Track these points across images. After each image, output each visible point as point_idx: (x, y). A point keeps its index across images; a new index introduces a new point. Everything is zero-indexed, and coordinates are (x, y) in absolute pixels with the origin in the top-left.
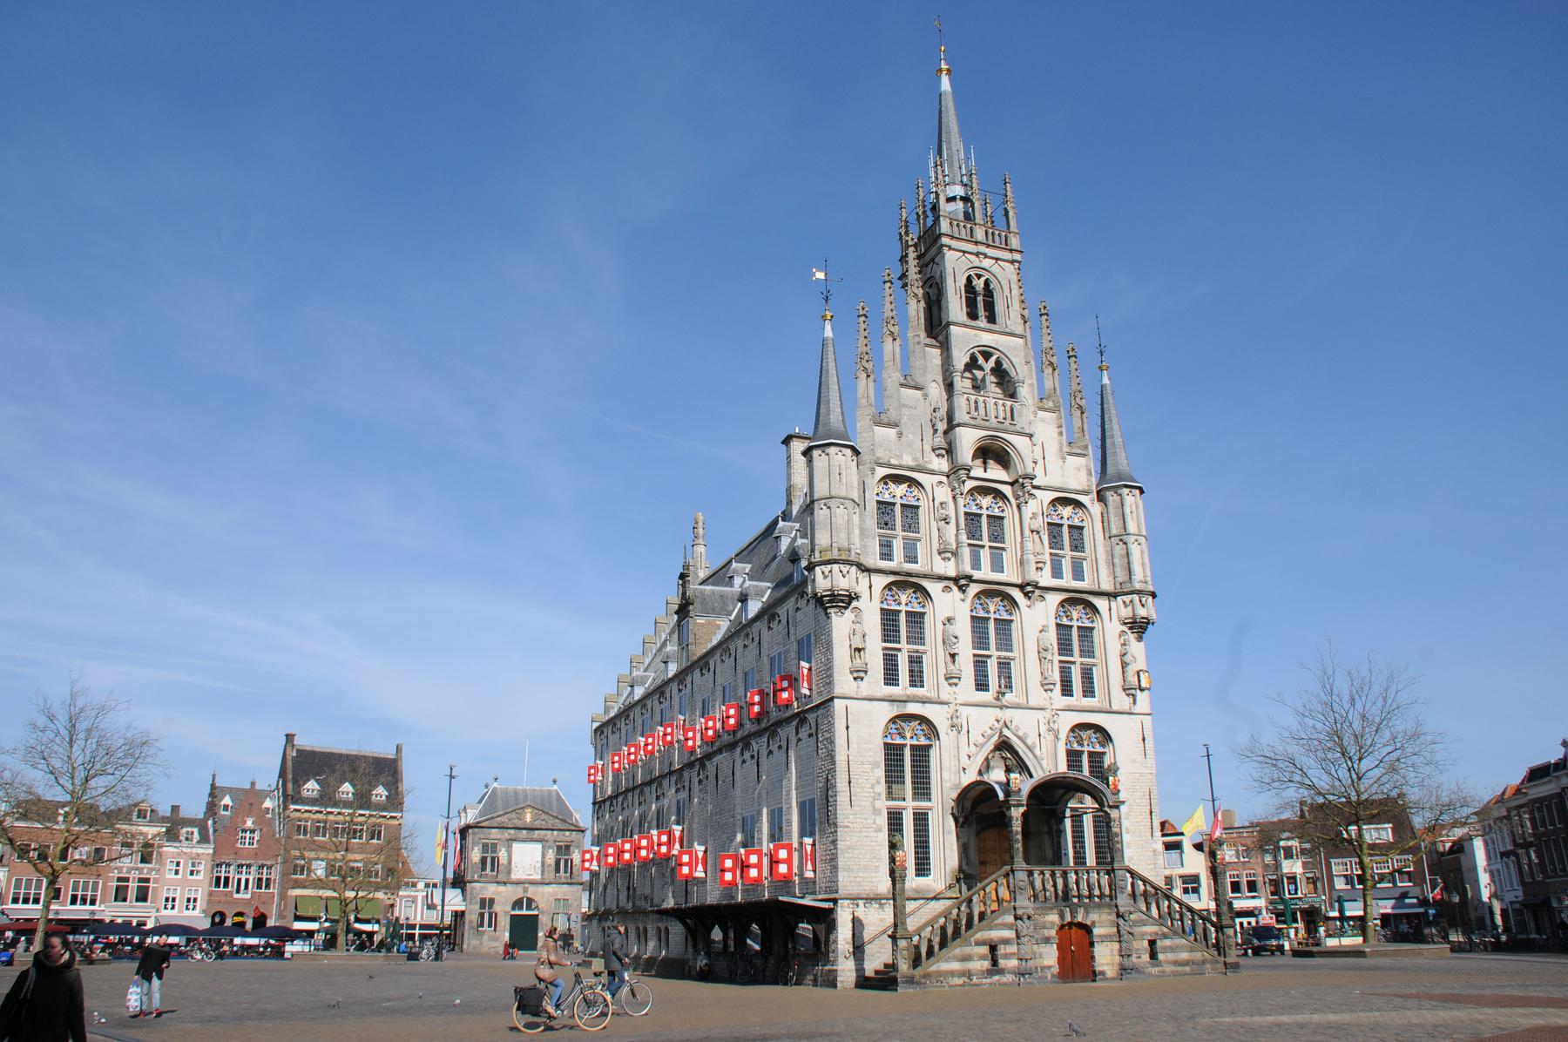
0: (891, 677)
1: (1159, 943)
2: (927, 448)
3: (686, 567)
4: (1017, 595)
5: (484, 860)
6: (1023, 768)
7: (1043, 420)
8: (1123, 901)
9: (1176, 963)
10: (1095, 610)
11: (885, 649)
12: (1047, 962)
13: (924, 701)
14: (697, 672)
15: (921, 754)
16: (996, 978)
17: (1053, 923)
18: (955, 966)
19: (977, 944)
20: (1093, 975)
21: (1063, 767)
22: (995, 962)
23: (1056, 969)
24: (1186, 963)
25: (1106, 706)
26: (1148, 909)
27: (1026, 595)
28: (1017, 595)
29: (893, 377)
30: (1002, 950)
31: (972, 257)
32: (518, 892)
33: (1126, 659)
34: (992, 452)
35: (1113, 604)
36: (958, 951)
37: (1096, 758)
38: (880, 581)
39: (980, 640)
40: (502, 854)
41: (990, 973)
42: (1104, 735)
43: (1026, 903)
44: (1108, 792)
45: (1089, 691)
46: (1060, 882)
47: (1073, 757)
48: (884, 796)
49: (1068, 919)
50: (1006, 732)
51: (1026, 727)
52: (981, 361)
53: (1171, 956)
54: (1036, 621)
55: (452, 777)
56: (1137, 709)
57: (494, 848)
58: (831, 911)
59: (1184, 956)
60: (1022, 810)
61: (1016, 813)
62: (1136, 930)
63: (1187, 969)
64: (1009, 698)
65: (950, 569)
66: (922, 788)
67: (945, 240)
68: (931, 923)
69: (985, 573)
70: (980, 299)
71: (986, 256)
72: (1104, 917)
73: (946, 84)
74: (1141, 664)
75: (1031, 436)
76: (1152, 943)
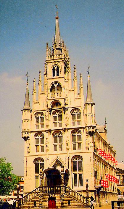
4: (62, 131)
9: (74, 205)
13: (41, 155)
18: (27, 205)
19: (32, 201)
20: (55, 207)
22: (35, 205)
23: (47, 206)
24: (77, 206)
28: (62, 131)
31: (53, 63)
34: (56, 103)
41: (34, 207)
43: (42, 193)
45: (80, 148)
46: (50, 189)
49: (50, 196)
54: (67, 136)
59: (76, 204)
76: (69, 201)
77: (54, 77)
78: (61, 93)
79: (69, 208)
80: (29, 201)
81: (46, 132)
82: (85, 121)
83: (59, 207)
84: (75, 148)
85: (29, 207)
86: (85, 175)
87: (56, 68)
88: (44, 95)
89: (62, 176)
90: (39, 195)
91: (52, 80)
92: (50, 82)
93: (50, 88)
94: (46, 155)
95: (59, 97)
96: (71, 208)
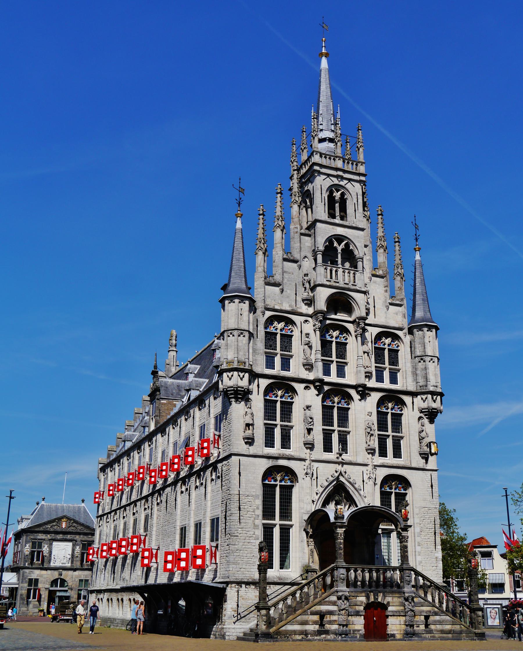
0: (269, 442)
1: (432, 618)
2: (299, 299)
3: (156, 367)
5: (32, 553)
6: (351, 501)
7: (375, 282)
8: (408, 590)
9: (442, 632)
10: (403, 403)
11: (265, 424)
12: (357, 627)
13: (289, 458)
14: (159, 435)
15: (287, 493)
16: (324, 636)
17: (362, 602)
19: (313, 613)
21: (377, 503)
22: (322, 625)
23: (363, 632)
24: (449, 632)
25: (408, 465)
26: (426, 595)
27: (358, 392)
29: (278, 253)
30: (328, 618)
32: (55, 575)
33: (423, 434)
34: (340, 302)
35: (415, 400)
36: (299, 618)
37: (401, 498)
38: (264, 383)
39: (327, 419)
40: (45, 549)
41: (319, 633)
42: (405, 483)
43: (345, 588)
44: (401, 520)
46: (367, 575)
47: (385, 496)
48: (261, 517)
49: (372, 599)
50: (341, 479)
51: (354, 474)
52: (336, 244)
53: (439, 627)
55: (11, 498)
56: (428, 467)
57: (40, 546)
58: (224, 590)
59: (448, 627)
60: (344, 529)
61: (341, 531)
62: (416, 609)
63: (450, 635)
64: (345, 457)
65: (311, 376)
66: (286, 514)
67: (316, 168)
68: (284, 599)
69: (333, 378)
70: (337, 205)
71: (342, 178)
72: (396, 599)
73: (324, 63)
74: (432, 438)
75: (365, 293)
76: (427, 618)
77: (332, 221)
78: (354, 274)
79: (430, 640)
80: (304, 613)
81: (304, 385)
82: (415, 374)
83: (398, 636)
84: (383, 453)
85: (305, 633)
86: (418, 539)
87: (337, 195)
88: (295, 265)
89: (341, 531)
90: (340, 594)
91: (331, 227)
92: (324, 232)
93: (322, 248)
94: (304, 460)
95: (350, 284)
96: (433, 638)
